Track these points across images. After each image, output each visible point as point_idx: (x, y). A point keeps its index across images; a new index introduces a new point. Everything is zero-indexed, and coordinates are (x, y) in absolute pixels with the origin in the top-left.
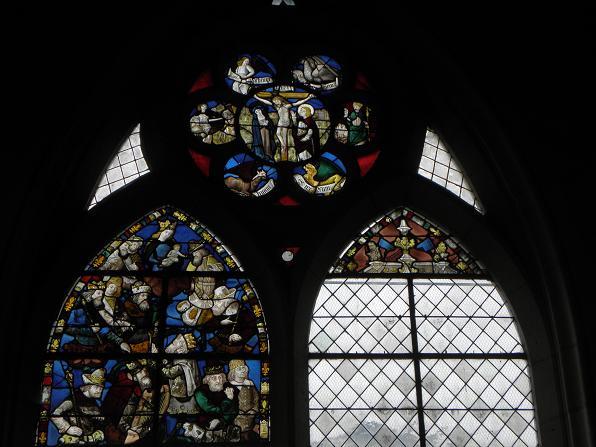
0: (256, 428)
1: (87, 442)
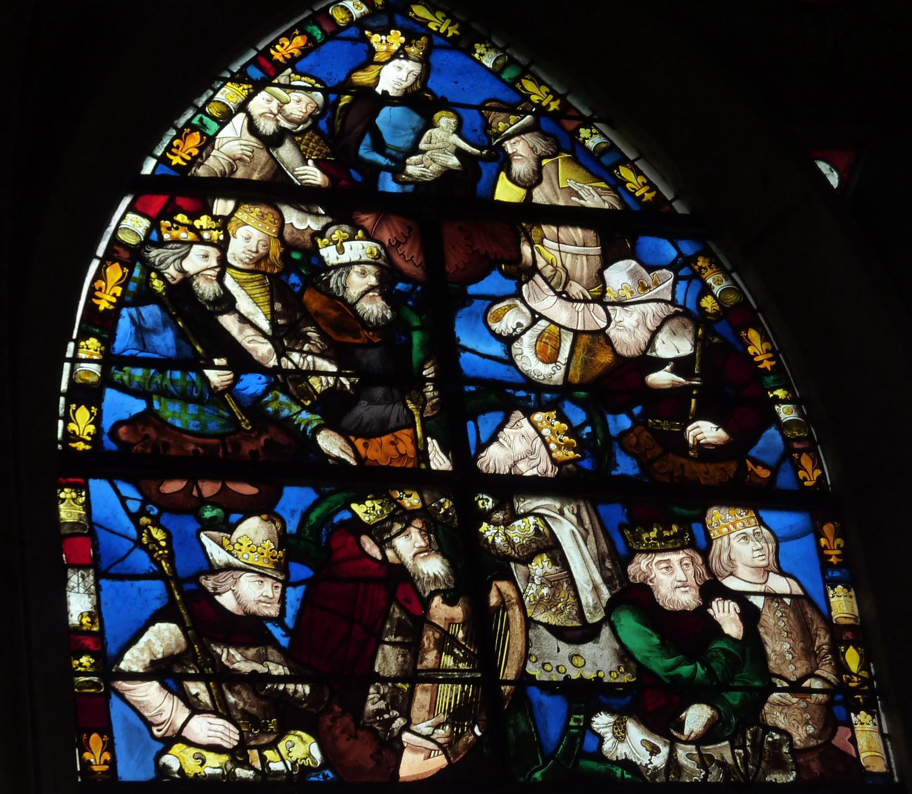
0: (841, 738)
1: (265, 773)
